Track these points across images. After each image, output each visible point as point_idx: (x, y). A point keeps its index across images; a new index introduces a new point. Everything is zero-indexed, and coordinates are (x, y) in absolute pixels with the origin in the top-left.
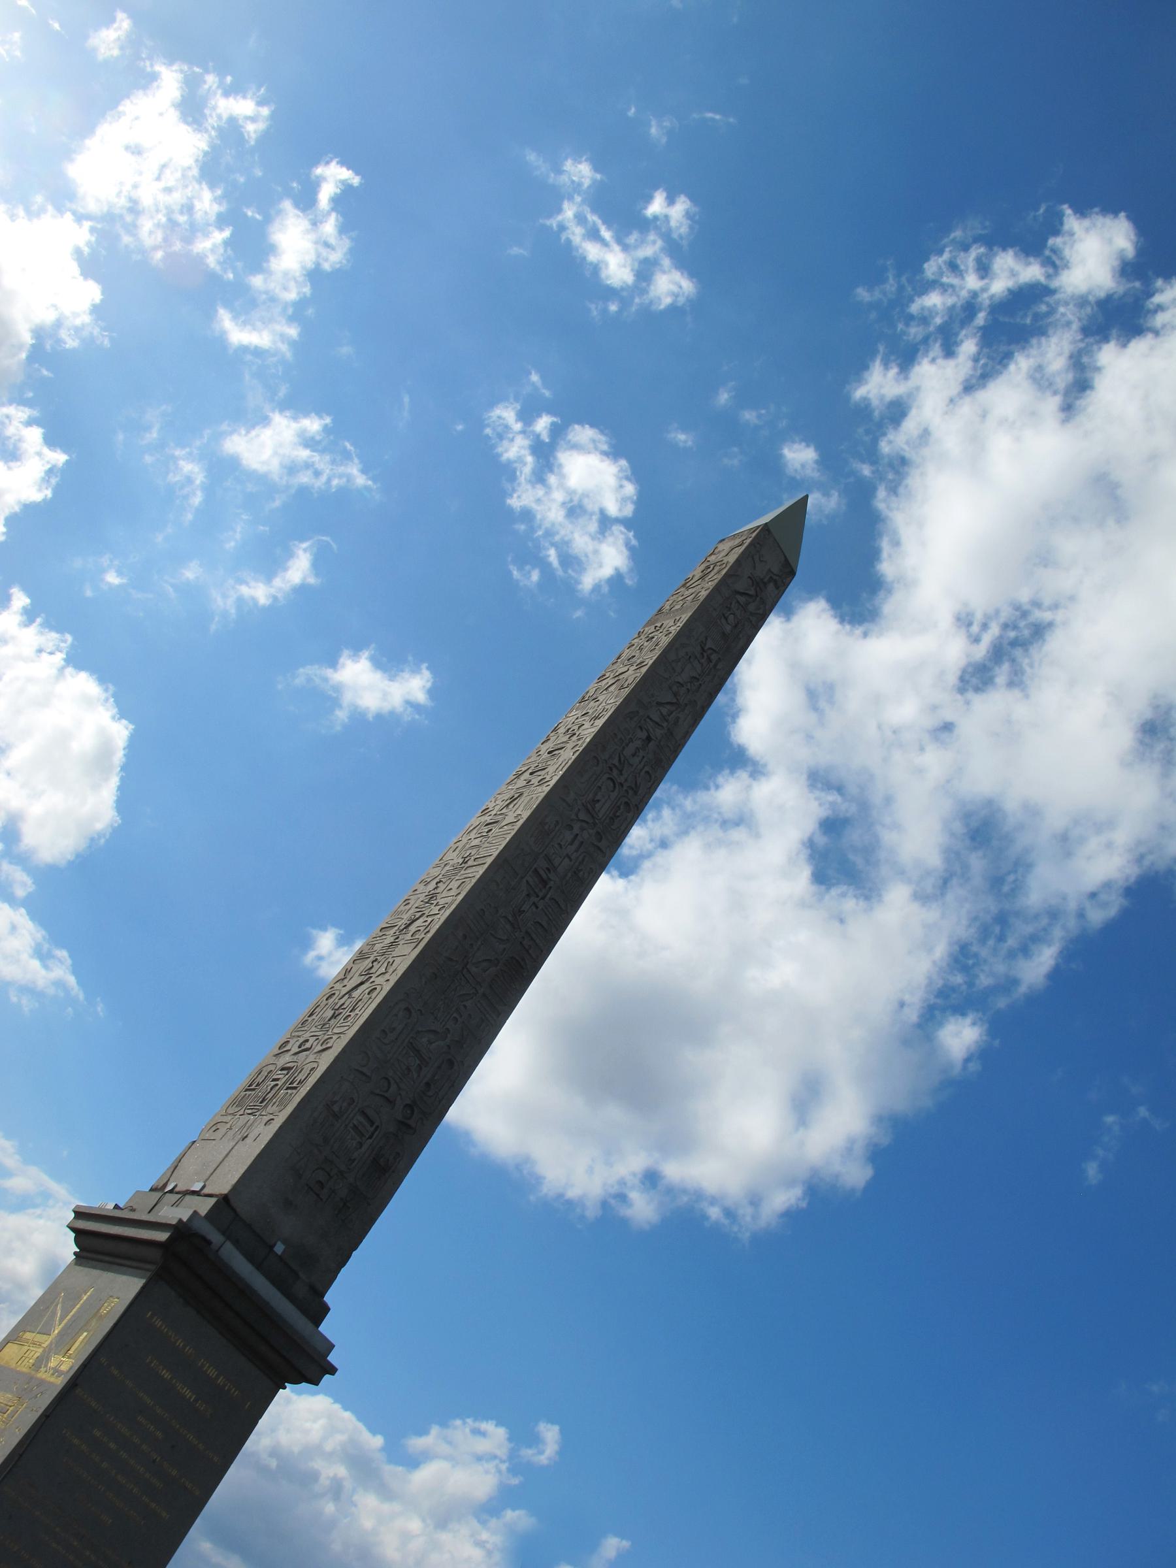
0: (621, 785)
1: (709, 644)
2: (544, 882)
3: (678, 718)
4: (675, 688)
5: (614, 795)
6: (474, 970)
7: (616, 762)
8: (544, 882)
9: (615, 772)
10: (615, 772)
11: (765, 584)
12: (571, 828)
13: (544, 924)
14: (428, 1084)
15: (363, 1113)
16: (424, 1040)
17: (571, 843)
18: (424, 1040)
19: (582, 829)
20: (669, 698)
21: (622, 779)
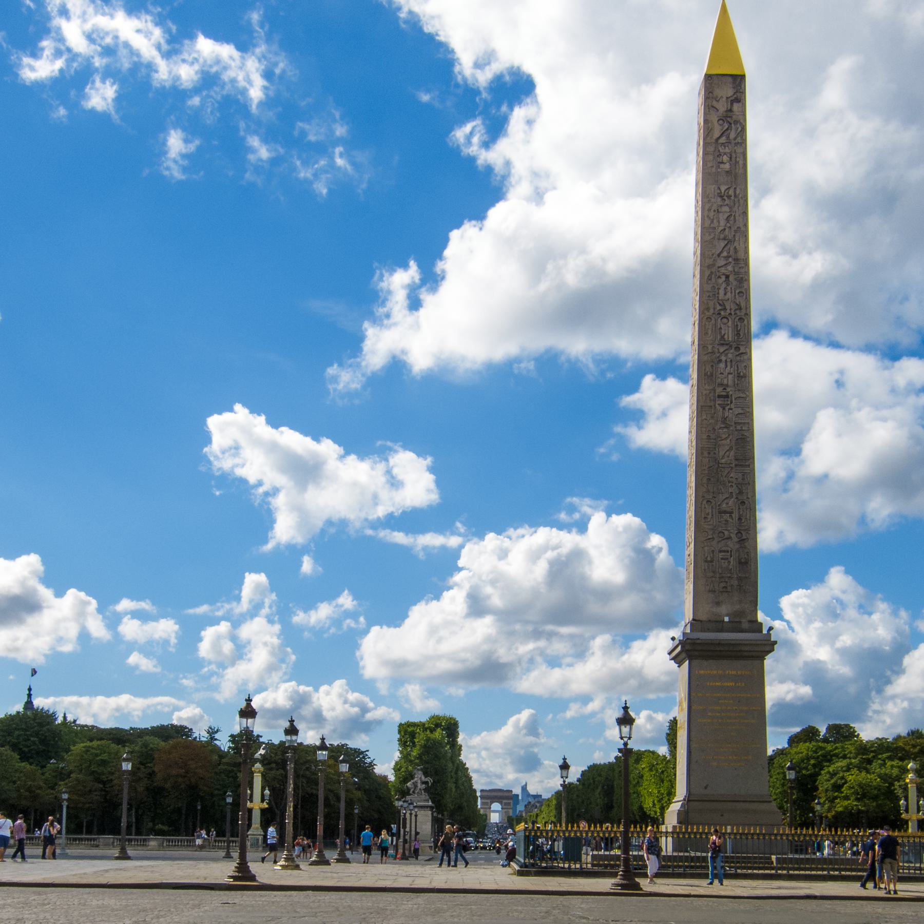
0: (730, 314)
1: (723, 188)
2: (727, 396)
3: (735, 248)
4: (722, 236)
5: (730, 324)
6: (723, 461)
7: (719, 308)
8: (727, 396)
9: (722, 313)
10: (722, 313)
11: (731, 111)
12: (720, 361)
13: (741, 411)
14: (740, 519)
15: (720, 551)
16: (724, 505)
17: (726, 366)
18: (724, 505)
19: (726, 355)
20: (723, 244)
21: (728, 311)
